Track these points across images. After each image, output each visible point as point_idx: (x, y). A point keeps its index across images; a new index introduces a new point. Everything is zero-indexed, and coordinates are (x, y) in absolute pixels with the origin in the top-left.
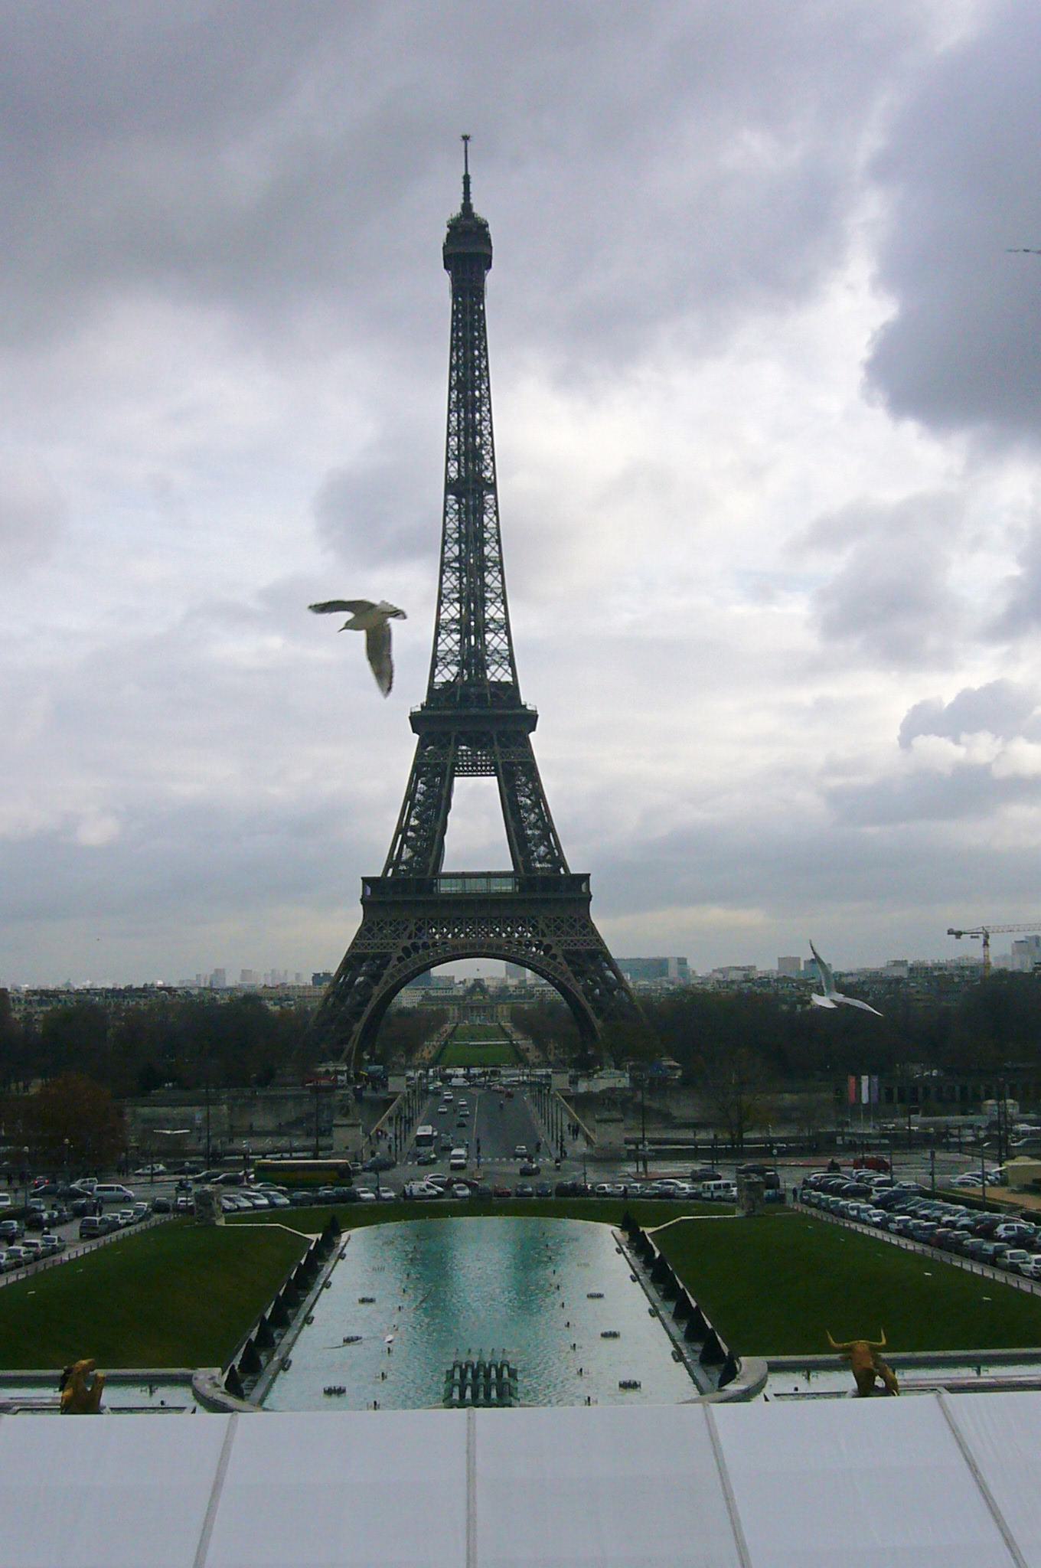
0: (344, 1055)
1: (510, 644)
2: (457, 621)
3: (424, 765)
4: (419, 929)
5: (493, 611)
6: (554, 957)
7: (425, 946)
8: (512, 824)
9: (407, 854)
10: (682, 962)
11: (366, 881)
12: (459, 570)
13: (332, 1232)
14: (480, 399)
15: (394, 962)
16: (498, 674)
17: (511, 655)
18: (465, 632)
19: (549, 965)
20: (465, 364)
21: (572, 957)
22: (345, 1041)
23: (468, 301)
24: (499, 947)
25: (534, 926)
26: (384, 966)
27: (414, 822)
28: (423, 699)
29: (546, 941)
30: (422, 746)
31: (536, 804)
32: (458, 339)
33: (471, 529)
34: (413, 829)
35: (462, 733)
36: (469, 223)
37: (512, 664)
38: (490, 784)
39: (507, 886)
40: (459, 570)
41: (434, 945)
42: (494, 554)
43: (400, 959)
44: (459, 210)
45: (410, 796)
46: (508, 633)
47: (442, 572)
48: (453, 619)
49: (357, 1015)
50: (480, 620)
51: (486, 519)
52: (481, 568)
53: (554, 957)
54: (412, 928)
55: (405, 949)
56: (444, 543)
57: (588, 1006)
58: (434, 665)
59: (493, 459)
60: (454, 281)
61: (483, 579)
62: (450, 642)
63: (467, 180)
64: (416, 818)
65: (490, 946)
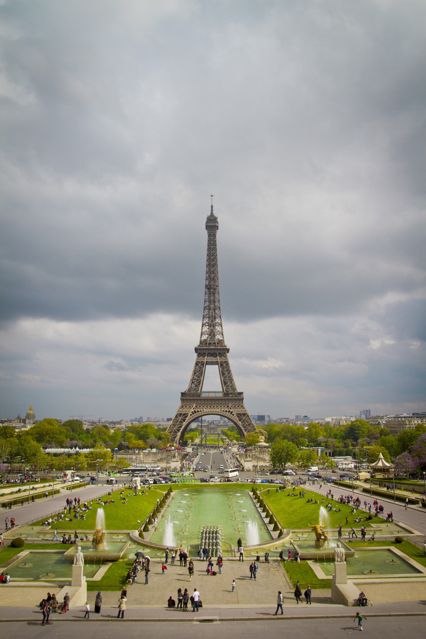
0: (175, 441)
1: (222, 329)
2: (208, 323)
3: (199, 362)
4: (197, 407)
5: (218, 320)
6: (233, 415)
7: (198, 411)
8: (222, 378)
9: (193, 385)
10: (268, 416)
11: (183, 394)
13: (170, 490)
15: (189, 416)
16: (219, 337)
17: (222, 332)
18: (210, 326)
19: (232, 417)
20: (211, 255)
21: (239, 415)
22: (175, 437)
23: (212, 238)
24: (218, 412)
25: (228, 407)
26: (187, 417)
27: (195, 377)
28: (198, 343)
29: (231, 410)
30: (198, 356)
31: (229, 373)
32: (209, 248)
33: (212, 298)
35: (209, 353)
36: (212, 218)
37: (222, 335)
39: (221, 395)
40: (209, 309)
41: (201, 411)
42: (218, 305)
43: (191, 415)
44: (209, 214)
46: (221, 326)
47: (204, 310)
48: (207, 323)
49: (179, 430)
50: (214, 323)
51: (216, 296)
52: (215, 310)
53: (233, 415)
54: (194, 406)
55: (192, 412)
56: (205, 302)
57: (243, 429)
58: (202, 335)
60: (208, 233)
61: (215, 311)
62: (206, 329)
63: (212, 207)
64: (196, 376)
65: (216, 412)
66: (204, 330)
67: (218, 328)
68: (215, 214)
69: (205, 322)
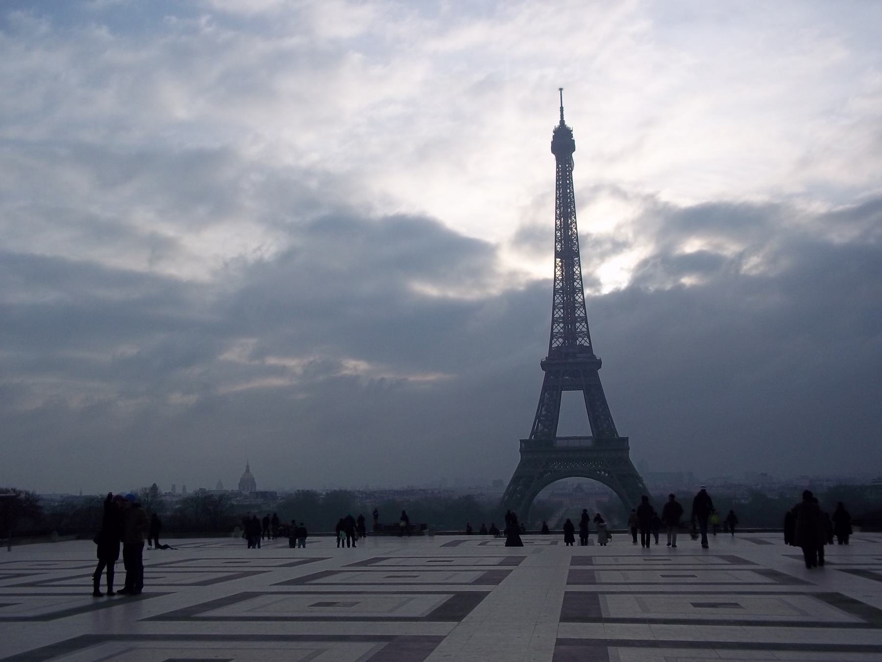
5: (579, 313)
12: (563, 293)
14: (571, 213)
16: (581, 341)
27: (544, 413)
34: (544, 416)
37: (589, 338)
38: (580, 393)
39: (589, 443)
40: (563, 293)
42: (578, 286)
44: (557, 124)
45: (541, 401)
46: (587, 323)
47: (555, 295)
59: (577, 240)
61: (574, 298)
62: (559, 328)
63: (562, 108)
66: (556, 330)
67: (580, 327)
68: (568, 123)
69: (557, 316)
